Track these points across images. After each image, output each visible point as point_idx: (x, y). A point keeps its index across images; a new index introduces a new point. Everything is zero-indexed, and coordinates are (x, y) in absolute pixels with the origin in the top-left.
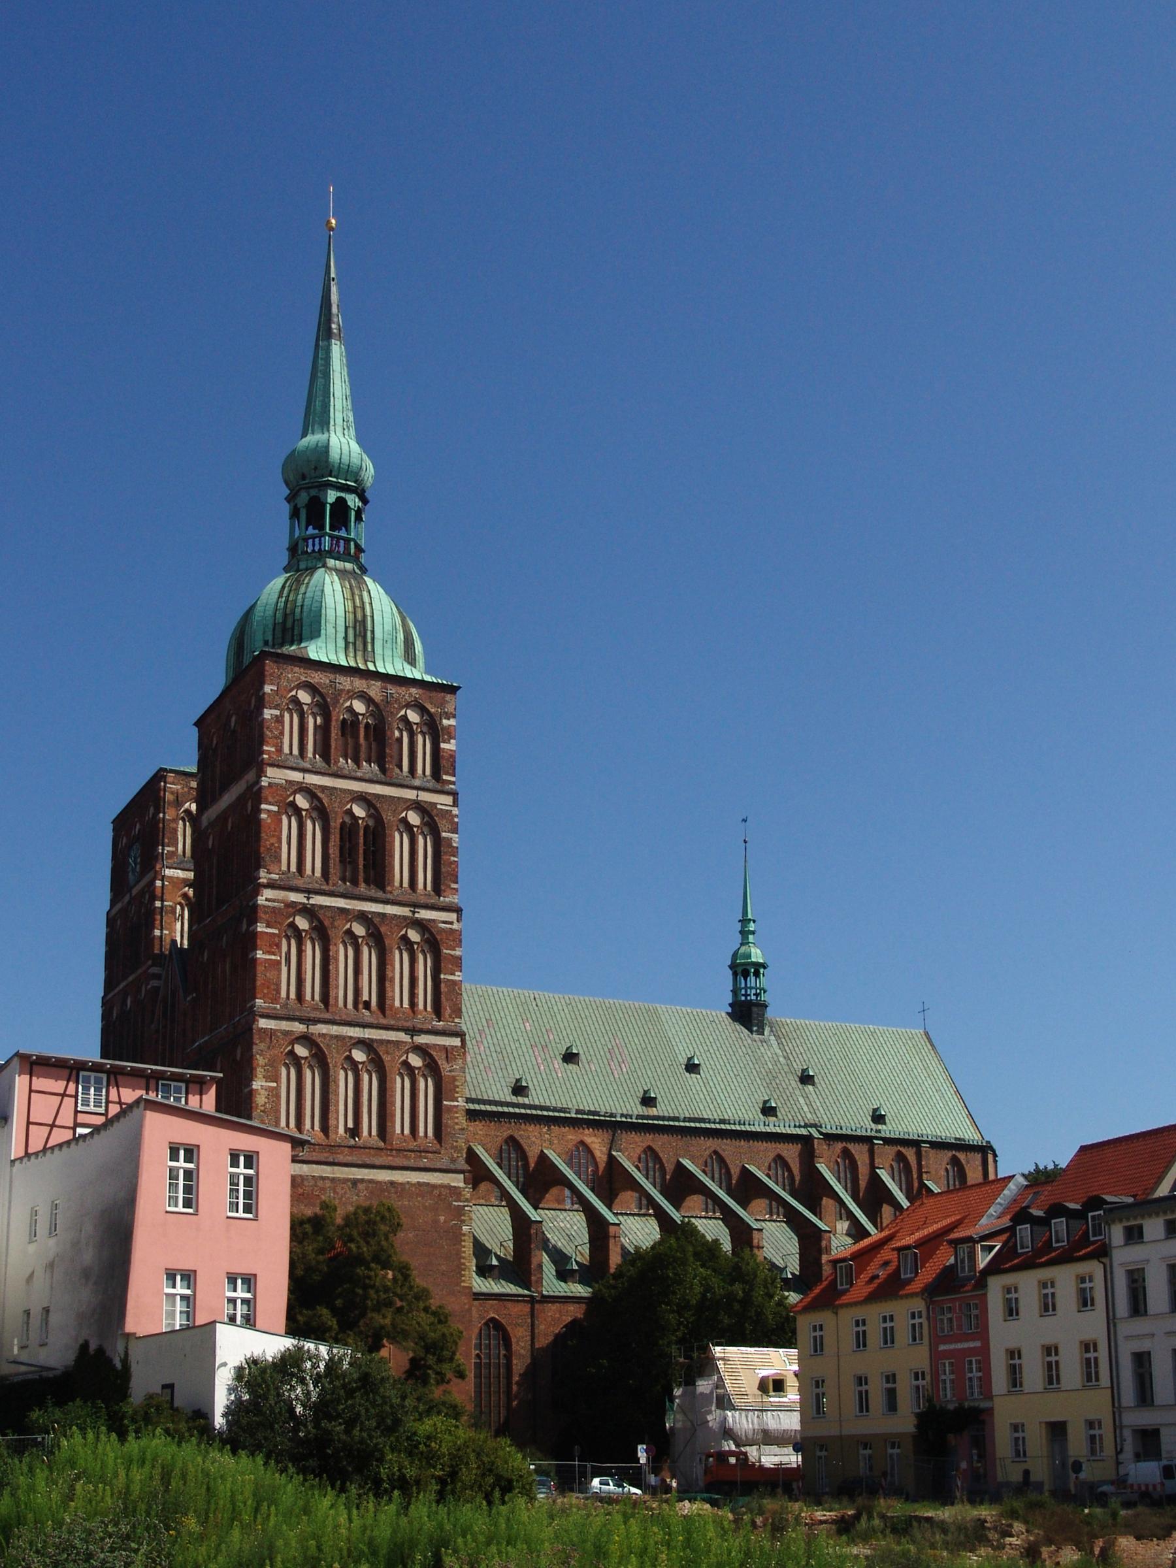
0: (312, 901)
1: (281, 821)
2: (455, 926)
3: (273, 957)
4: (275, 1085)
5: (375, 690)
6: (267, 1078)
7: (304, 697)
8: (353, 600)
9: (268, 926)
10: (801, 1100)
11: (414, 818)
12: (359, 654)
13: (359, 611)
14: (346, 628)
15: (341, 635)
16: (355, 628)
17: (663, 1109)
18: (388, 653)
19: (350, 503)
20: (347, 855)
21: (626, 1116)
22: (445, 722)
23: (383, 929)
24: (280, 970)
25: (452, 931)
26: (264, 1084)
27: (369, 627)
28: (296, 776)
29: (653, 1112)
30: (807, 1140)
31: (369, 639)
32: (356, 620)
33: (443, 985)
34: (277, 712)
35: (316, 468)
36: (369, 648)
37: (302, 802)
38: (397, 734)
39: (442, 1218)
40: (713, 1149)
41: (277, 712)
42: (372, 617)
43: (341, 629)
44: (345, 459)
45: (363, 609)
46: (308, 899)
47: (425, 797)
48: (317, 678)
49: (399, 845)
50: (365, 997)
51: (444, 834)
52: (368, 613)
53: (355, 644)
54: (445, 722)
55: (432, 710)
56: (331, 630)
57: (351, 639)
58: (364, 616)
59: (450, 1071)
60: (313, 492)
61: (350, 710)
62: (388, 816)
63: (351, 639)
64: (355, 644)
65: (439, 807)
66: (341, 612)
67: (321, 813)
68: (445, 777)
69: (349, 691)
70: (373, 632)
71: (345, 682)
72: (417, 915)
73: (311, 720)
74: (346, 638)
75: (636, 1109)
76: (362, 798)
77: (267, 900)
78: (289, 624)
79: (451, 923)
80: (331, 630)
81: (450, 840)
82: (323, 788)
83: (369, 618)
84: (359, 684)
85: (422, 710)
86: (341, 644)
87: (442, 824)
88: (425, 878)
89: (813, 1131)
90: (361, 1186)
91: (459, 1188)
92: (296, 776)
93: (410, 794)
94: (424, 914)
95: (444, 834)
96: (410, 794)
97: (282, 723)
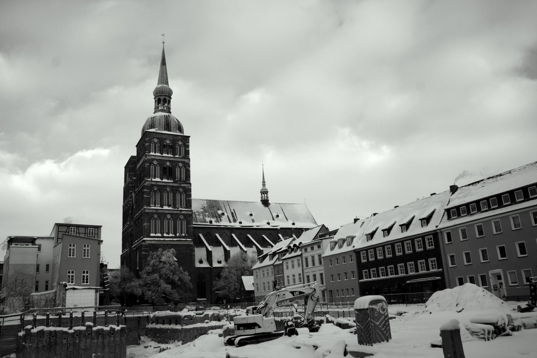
0: (157, 184)
1: (150, 167)
2: (190, 188)
3: (148, 196)
4: (149, 224)
6: (148, 223)
7: (156, 140)
9: (147, 190)
11: (180, 165)
14: (165, 125)
15: (164, 127)
16: (167, 125)
24: (150, 199)
26: (147, 224)
27: (170, 125)
32: (167, 123)
33: (187, 200)
34: (149, 144)
35: (159, 92)
36: (170, 129)
38: (176, 147)
39: (188, 251)
41: (149, 144)
43: (164, 125)
46: (156, 183)
50: (170, 204)
51: (187, 168)
57: (166, 127)
59: (189, 219)
60: (159, 97)
64: (167, 129)
66: (163, 122)
67: (160, 165)
69: (165, 139)
70: (171, 126)
73: (157, 145)
77: (147, 184)
78: (153, 125)
79: (189, 187)
85: (182, 141)
90: (169, 245)
91: (191, 244)
94: (183, 185)
97: (150, 147)
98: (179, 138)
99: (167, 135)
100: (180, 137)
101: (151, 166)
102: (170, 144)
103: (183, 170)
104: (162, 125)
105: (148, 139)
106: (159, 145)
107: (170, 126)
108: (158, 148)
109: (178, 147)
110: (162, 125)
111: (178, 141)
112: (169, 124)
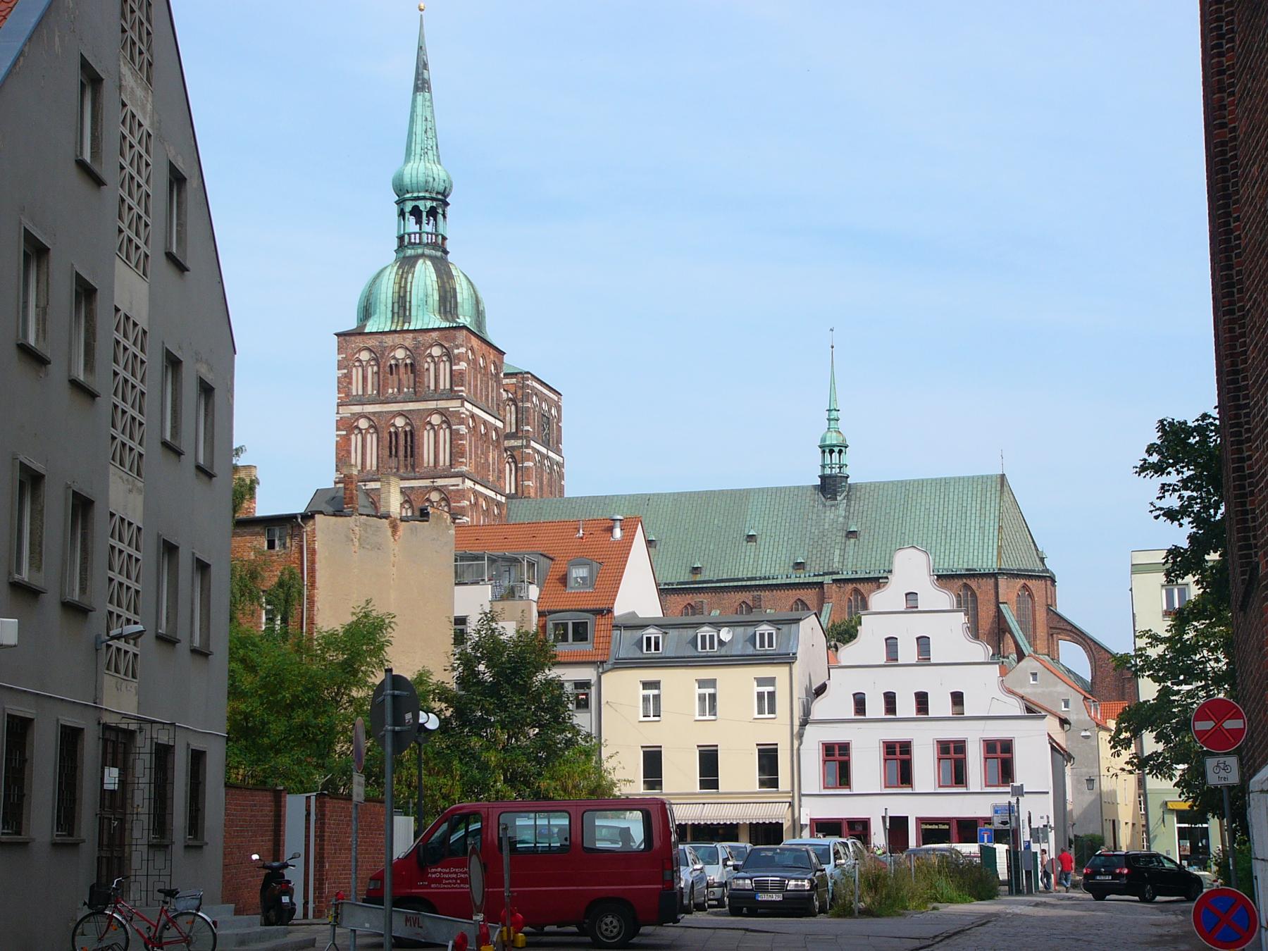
1: (350, 440)
2: (460, 487)
5: (408, 340)
7: (365, 356)
8: (400, 283)
10: (837, 552)
11: (436, 419)
12: (401, 319)
13: (402, 289)
14: (393, 303)
15: (390, 309)
16: (398, 302)
17: (705, 575)
18: (420, 313)
19: (422, 208)
20: (393, 451)
21: (668, 584)
22: (456, 351)
23: (412, 497)
25: (458, 491)
27: (408, 300)
28: (357, 409)
29: (699, 578)
30: (821, 585)
31: (408, 307)
32: (399, 296)
34: (345, 371)
36: (408, 314)
37: (363, 424)
38: (426, 366)
40: (741, 601)
41: (345, 371)
42: (411, 292)
43: (390, 305)
44: (414, 181)
45: (405, 287)
47: (442, 404)
48: (371, 342)
49: (427, 438)
51: (454, 427)
52: (408, 289)
53: (398, 313)
54: (456, 351)
55: (447, 346)
56: (383, 308)
57: (396, 310)
58: (406, 292)
61: (394, 358)
62: (417, 423)
63: (396, 310)
64: (398, 313)
65: (451, 409)
66: (390, 294)
68: (456, 389)
70: (410, 302)
71: (389, 340)
72: (435, 484)
74: (393, 311)
75: (685, 576)
76: (400, 414)
79: (458, 485)
80: (383, 308)
81: (458, 430)
82: (374, 413)
83: (408, 293)
84: (397, 339)
85: (442, 346)
86: (390, 315)
87: (453, 420)
88: (444, 458)
89: (827, 579)
92: (357, 409)
93: (432, 405)
94: (440, 482)
95: (454, 427)
96: (432, 405)
98: (433, 339)
99: (397, 335)
100: (434, 335)
101: (353, 437)
102: (408, 361)
103: (444, 435)
104: (386, 305)
105: (344, 356)
106: (375, 369)
107: (408, 304)
108: (373, 378)
109: (432, 365)
110: (386, 305)
111: (431, 346)
112: (405, 296)
